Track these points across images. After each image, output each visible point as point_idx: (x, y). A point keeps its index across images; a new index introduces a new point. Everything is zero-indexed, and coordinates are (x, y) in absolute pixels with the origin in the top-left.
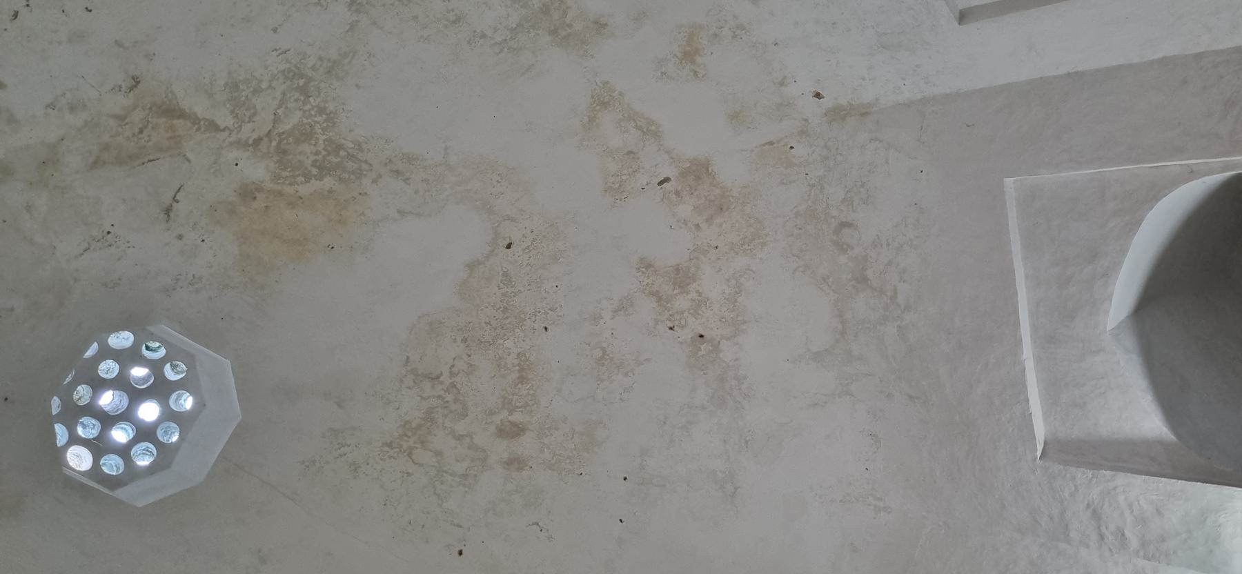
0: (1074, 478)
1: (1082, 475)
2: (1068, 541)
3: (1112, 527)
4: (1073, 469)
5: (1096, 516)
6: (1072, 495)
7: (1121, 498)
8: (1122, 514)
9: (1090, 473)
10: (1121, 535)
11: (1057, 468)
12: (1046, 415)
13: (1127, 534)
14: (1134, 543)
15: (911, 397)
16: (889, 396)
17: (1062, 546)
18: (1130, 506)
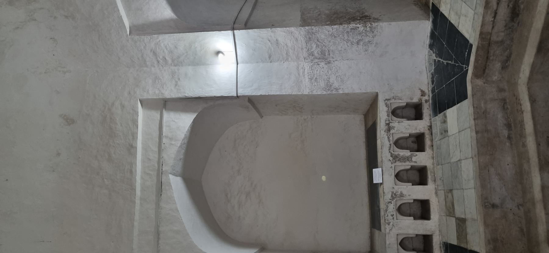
0: (144, 40)
1: (146, 38)
2: (147, 66)
3: (161, 57)
4: (143, 37)
5: (155, 54)
6: (145, 47)
7: (162, 45)
8: (163, 51)
9: (149, 37)
10: (164, 59)
11: (136, 37)
12: (128, 15)
13: (167, 58)
14: (170, 61)
15: (67, 17)
16: (55, 18)
17: (145, 68)
18: (166, 47)
